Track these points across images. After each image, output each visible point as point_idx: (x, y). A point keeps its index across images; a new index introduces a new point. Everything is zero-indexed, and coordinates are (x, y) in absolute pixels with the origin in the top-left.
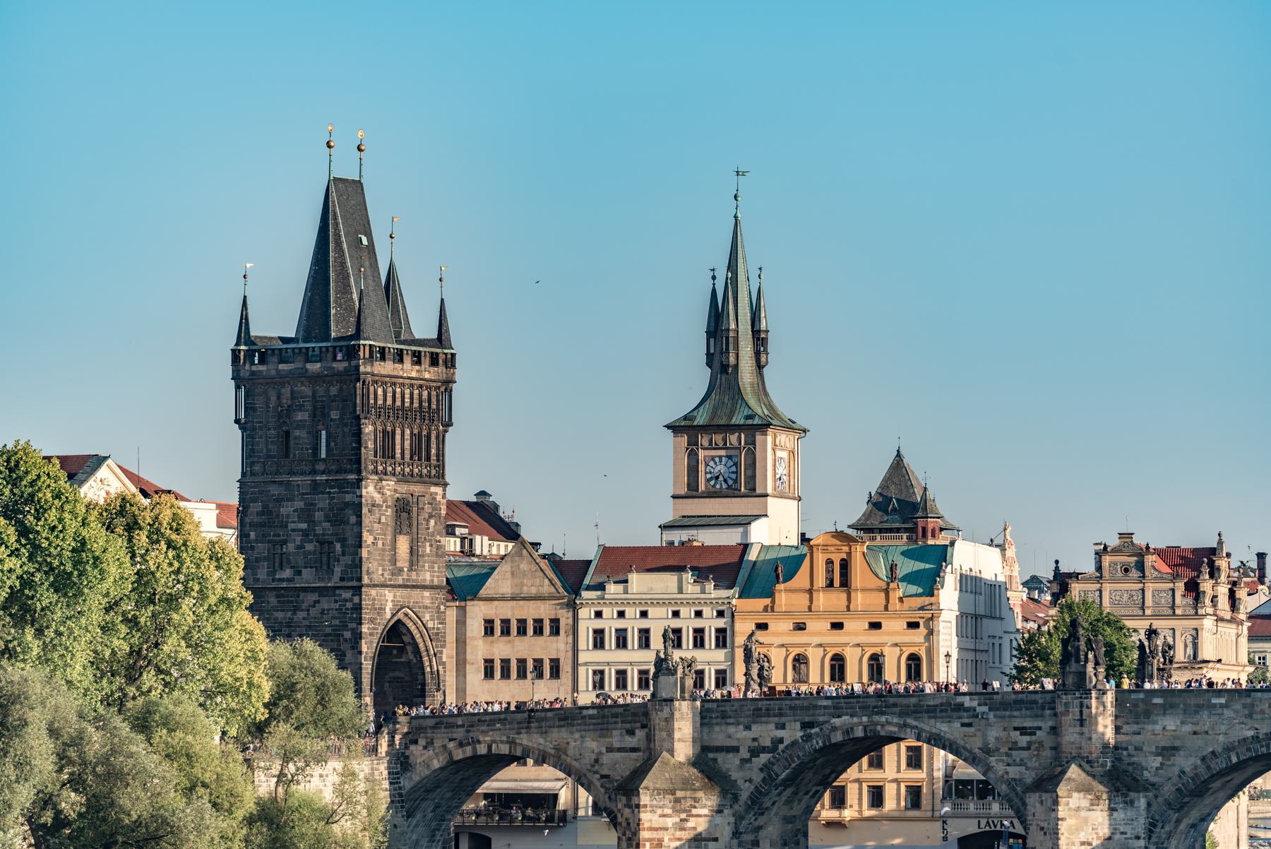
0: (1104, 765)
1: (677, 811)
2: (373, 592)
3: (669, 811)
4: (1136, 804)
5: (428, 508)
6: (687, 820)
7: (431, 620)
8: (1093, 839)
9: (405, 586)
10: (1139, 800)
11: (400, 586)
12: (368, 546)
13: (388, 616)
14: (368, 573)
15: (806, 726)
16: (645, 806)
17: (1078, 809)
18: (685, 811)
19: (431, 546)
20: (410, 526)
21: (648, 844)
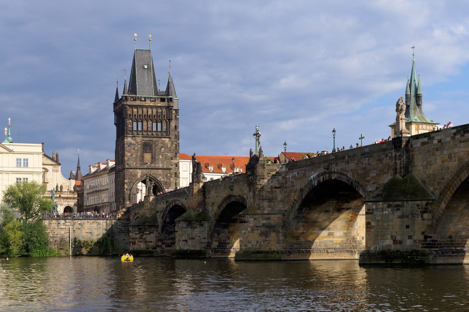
0: (198, 211)
1: (140, 233)
2: (131, 170)
3: (137, 233)
4: (204, 225)
5: (160, 145)
6: (143, 236)
7: (162, 178)
8: (188, 239)
9: (147, 169)
10: (205, 224)
11: (144, 169)
12: (128, 156)
13: (139, 176)
14: (128, 164)
15: (167, 202)
16: (131, 231)
17: (182, 227)
18: (142, 232)
19: (162, 156)
20: (151, 149)
21: (131, 243)
